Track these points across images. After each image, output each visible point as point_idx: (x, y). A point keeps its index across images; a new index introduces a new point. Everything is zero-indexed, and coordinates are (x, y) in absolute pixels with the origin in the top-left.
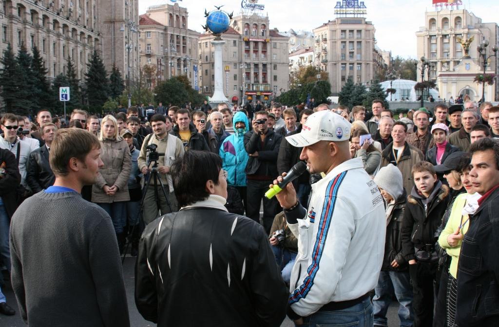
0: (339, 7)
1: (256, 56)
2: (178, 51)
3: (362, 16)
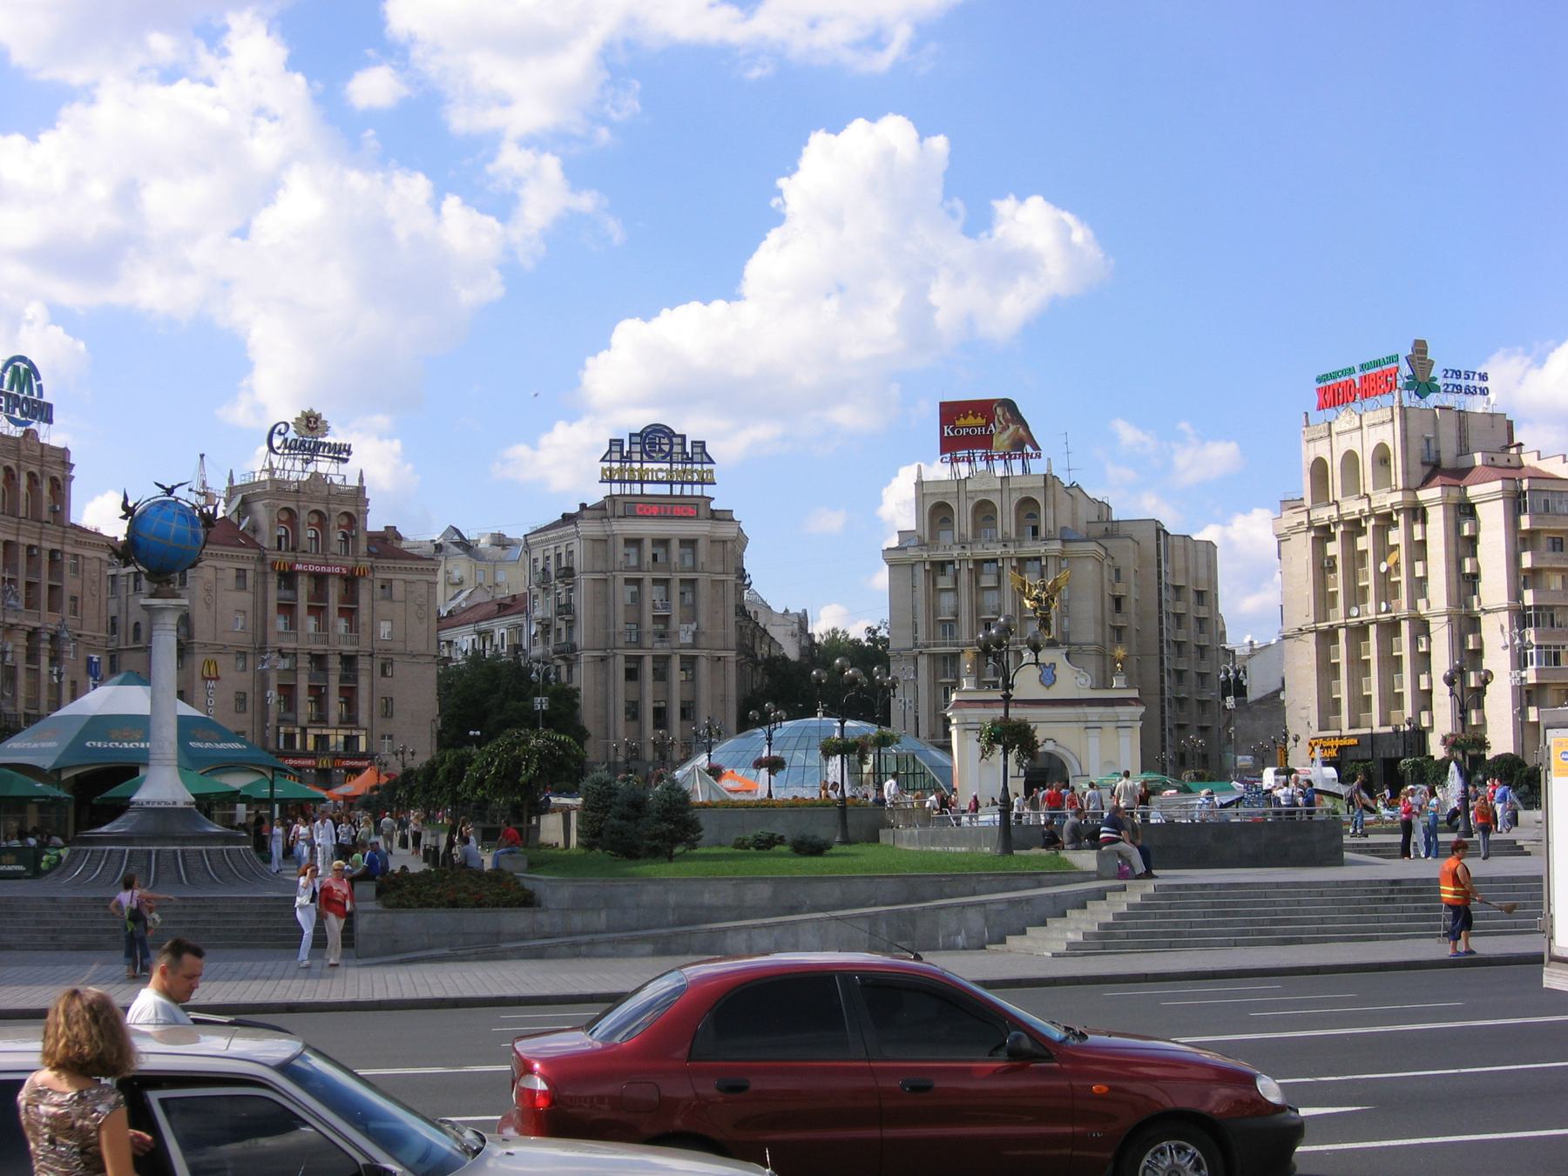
0: (617, 456)
1: (318, 628)
2: (31, 604)
3: (697, 490)
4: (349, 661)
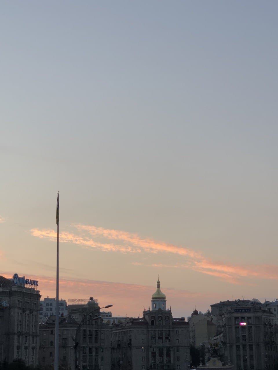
4: (169, 350)
